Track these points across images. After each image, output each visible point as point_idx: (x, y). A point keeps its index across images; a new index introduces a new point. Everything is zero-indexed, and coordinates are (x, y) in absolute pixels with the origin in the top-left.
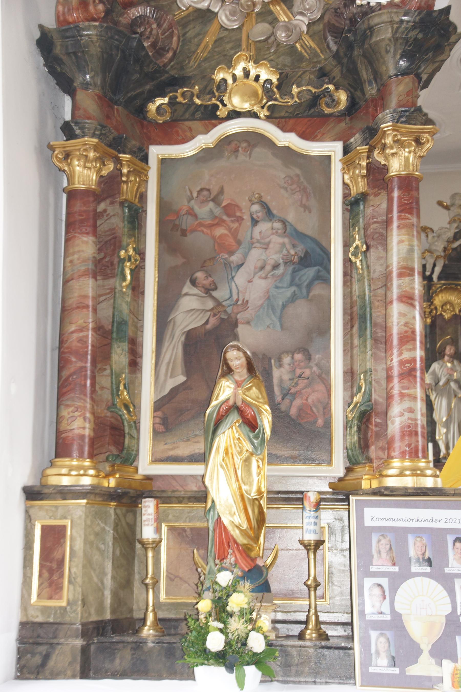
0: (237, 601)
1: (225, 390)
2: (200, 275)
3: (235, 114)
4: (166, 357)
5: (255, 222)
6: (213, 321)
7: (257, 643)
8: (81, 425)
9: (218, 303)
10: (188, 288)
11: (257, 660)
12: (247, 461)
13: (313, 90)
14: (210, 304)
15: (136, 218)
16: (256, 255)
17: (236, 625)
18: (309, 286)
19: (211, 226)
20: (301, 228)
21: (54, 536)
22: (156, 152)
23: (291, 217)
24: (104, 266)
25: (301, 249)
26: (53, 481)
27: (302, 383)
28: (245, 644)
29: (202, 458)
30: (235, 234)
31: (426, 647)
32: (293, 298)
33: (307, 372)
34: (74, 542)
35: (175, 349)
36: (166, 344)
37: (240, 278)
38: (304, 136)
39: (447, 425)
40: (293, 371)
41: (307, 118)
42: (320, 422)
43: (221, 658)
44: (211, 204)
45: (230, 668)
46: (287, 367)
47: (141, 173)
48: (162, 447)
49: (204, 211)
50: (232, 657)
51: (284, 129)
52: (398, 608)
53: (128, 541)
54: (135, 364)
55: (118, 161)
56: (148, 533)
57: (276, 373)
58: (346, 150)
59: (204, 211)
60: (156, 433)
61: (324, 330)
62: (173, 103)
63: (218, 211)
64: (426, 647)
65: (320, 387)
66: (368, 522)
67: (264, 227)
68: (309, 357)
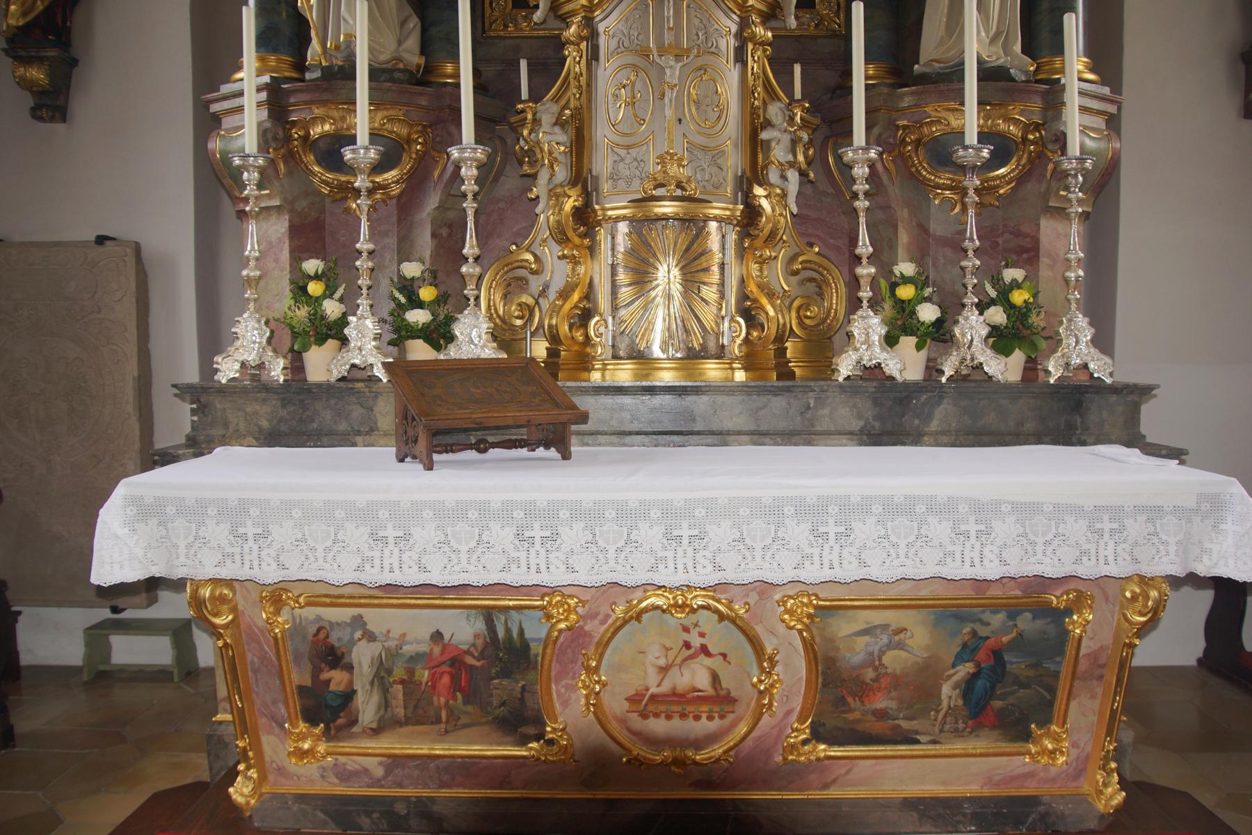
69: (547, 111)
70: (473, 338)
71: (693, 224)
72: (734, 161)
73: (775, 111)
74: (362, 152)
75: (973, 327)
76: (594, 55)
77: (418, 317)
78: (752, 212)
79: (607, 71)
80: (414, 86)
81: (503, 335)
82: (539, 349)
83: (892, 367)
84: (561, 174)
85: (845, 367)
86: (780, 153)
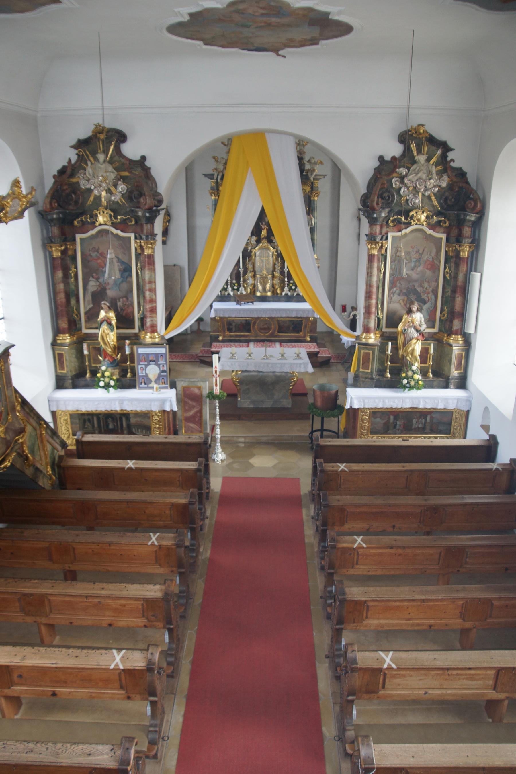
0: (107, 374)
1: (103, 314)
2: (94, 275)
3: (100, 225)
4: (87, 299)
6: (99, 289)
7: (112, 383)
8: (64, 324)
9: (101, 283)
10: (91, 279)
13: (124, 218)
14: (98, 283)
15: (74, 258)
17: (107, 380)
18: (127, 278)
19: (96, 260)
20: (123, 260)
21: (61, 356)
24: (66, 276)
25: (123, 267)
26: (59, 342)
27: (126, 306)
28: (109, 383)
32: (122, 282)
33: (127, 303)
34: (66, 357)
35: (89, 297)
36: (86, 295)
38: (123, 231)
40: (123, 303)
41: (123, 226)
42: (132, 317)
43: (103, 387)
44: (96, 253)
45: (106, 389)
46: (121, 302)
48: (89, 325)
49: (94, 254)
50: (107, 386)
51: (117, 229)
52: (147, 372)
53: (80, 351)
54: (78, 301)
55: (66, 245)
59: (94, 254)
60: (86, 321)
61: (131, 291)
63: (98, 255)
65: (131, 307)
66: (139, 352)
68: (127, 299)
69: (250, 263)
70: (242, 291)
72: (271, 269)
73: (277, 263)
76: (255, 256)
77: (235, 288)
78: (273, 274)
79: (258, 258)
83: (289, 294)
84: (252, 270)
85: (283, 294)
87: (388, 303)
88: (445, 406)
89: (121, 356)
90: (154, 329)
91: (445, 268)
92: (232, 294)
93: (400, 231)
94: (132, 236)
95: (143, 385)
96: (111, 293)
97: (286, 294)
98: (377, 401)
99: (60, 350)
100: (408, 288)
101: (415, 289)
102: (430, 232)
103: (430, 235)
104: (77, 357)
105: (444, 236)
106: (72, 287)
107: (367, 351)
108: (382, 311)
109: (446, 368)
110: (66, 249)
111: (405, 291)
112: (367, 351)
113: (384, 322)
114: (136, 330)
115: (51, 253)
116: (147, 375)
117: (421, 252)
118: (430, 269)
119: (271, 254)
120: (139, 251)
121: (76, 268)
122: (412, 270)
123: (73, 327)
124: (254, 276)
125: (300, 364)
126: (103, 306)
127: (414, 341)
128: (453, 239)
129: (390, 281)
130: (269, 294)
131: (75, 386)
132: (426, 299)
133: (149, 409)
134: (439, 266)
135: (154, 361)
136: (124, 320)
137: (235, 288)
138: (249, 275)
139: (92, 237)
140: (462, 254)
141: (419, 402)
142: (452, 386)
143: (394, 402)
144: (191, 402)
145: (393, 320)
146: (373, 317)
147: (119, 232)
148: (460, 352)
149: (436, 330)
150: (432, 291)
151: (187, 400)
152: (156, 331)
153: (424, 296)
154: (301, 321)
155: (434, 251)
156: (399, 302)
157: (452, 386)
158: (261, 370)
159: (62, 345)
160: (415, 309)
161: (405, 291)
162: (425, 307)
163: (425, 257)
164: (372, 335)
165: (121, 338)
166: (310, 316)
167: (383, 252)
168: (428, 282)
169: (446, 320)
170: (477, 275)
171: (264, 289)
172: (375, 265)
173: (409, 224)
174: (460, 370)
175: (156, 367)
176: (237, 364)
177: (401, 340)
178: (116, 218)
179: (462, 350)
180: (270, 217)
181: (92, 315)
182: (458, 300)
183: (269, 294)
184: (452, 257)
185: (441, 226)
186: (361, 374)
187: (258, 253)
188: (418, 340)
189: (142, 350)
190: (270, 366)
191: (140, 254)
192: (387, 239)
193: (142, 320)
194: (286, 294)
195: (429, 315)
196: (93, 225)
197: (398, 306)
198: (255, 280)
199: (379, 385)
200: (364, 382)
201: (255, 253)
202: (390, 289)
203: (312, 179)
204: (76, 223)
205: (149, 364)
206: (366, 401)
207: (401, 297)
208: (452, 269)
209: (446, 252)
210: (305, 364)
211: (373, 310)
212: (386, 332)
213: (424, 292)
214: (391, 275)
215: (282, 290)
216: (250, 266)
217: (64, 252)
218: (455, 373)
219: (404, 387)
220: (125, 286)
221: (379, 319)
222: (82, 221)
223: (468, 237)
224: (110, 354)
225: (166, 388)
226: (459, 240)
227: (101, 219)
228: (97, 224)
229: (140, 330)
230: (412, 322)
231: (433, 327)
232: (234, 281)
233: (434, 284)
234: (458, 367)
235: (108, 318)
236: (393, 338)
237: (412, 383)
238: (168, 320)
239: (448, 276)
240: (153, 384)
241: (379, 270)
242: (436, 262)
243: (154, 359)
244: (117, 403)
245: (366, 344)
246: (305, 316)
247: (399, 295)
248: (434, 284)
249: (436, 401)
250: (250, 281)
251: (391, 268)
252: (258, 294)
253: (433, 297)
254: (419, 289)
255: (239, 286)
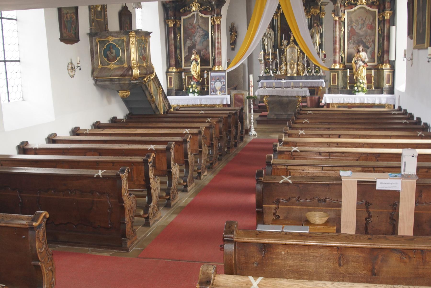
0: (194, 86)
1: (193, 57)
3: (194, 11)
5: (198, 29)
7: (196, 91)
8: (173, 62)
9: (193, 42)
10: (188, 40)
11: (197, 93)
12: (196, 67)
16: (198, 34)
17: (194, 89)
20: (205, 30)
21: (170, 78)
22: (183, 18)
23: (203, 28)
25: (205, 33)
26: (170, 71)
29: (190, 66)
30: (195, 31)
31: (218, 90)
34: (173, 79)
35: (187, 49)
37: (196, 38)
38: (205, 14)
39: (267, 45)
41: (205, 12)
43: (192, 93)
47: (180, 22)
49: (190, 27)
50: (193, 92)
51: (202, 13)
56: (183, 77)
57: (202, 53)
58: (211, 17)
59: (190, 27)
62: (184, 10)
64: (218, 90)
67: (199, 29)
70: (279, 73)
71: (294, 65)
72: (297, 60)
74: (271, 60)
75: (313, 71)
77: (275, 71)
79: (288, 54)
80: (274, 55)
81: (280, 73)
82: (283, 73)
83: (308, 75)
85: (304, 75)
86: (300, 60)
87: (348, 49)
88: (380, 102)
89: (202, 81)
90: (220, 64)
91: (378, 28)
92: (272, 75)
93: (352, 8)
94: (210, 17)
95: (213, 93)
96: (198, 47)
97: (306, 75)
98: (340, 99)
99: (170, 75)
100: (358, 40)
101: (362, 41)
102: (368, 8)
103: (369, 10)
104: (179, 80)
105: (376, 10)
106: (178, 43)
107: (335, 73)
108: (344, 53)
109: (381, 84)
110: (176, 23)
111: (356, 42)
112: (335, 73)
113: (345, 59)
114: (211, 67)
115: (168, 25)
116: (215, 87)
117: (364, 19)
118: (370, 29)
119: (296, 50)
120: (213, 24)
121: (181, 34)
122: (360, 29)
123: (178, 64)
124: (286, 65)
125: (302, 91)
126: (193, 52)
127: (361, 68)
128: (381, 11)
129: (348, 36)
130: (295, 75)
131: (177, 94)
132: (369, 46)
133: (215, 104)
134: (375, 27)
135: (218, 80)
136: (204, 62)
137: (275, 71)
138: (284, 64)
139: (189, 18)
140: (386, 18)
141: (364, 100)
142: (385, 93)
143: (349, 100)
144: (238, 103)
145: (350, 58)
146: (337, 54)
147: (204, 16)
148: (388, 73)
149: (376, 63)
150: (372, 41)
151: (236, 102)
152: (221, 65)
153: (368, 44)
154: (315, 89)
155: (372, 19)
156: (353, 48)
157: (385, 93)
158: (280, 95)
159: (171, 72)
160: (361, 49)
161: (356, 42)
162: (369, 51)
163: (367, 22)
164: (337, 64)
165: (202, 71)
166: (319, 86)
167: (342, 20)
168: (369, 36)
169: (380, 57)
170: (393, 28)
171: (292, 72)
172: (337, 26)
173: (356, 5)
174: (390, 83)
175: (220, 83)
176: (266, 92)
177: (354, 68)
178: (201, 7)
179: (390, 72)
180: (283, 8)
181: (188, 60)
182: (386, 43)
183: (295, 75)
184: (381, 21)
185: (374, 5)
186: (332, 87)
187: (288, 51)
188: (364, 67)
189: (213, 74)
190: (285, 92)
191: (213, 25)
192: (344, 13)
193: (214, 60)
194: (306, 75)
195: (371, 55)
196: (190, 11)
197: (353, 51)
198: (287, 67)
199: (342, 92)
200: (333, 91)
201: (286, 51)
202: (348, 41)
203: (320, 4)
204: (181, 10)
205: (216, 82)
206: (334, 99)
207: (355, 45)
208: (382, 27)
209: (379, 19)
210: (305, 92)
211: (338, 50)
212: (347, 66)
213: (368, 42)
214: (348, 33)
215: (303, 73)
216: (283, 59)
217: (174, 25)
218: (386, 85)
219: (356, 91)
220: (205, 43)
221: (342, 57)
222: (184, 10)
223: (388, 8)
224: (196, 78)
225: (225, 94)
226: (384, 11)
227: (194, 9)
228: (192, 11)
229: (212, 67)
230: (360, 57)
231: (374, 62)
232: (274, 68)
233: (373, 37)
234: (388, 82)
235: (196, 58)
236: (351, 69)
237: (360, 89)
238: (228, 64)
239: (380, 32)
240: (218, 92)
241: (340, 29)
242: (373, 25)
243: (219, 79)
244: (198, 100)
245: (334, 69)
246: (316, 86)
247: (353, 44)
248: (373, 37)
249: (374, 99)
250: (284, 68)
251: (348, 29)
252: (289, 75)
253: (373, 45)
254: (364, 41)
255: (277, 70)
